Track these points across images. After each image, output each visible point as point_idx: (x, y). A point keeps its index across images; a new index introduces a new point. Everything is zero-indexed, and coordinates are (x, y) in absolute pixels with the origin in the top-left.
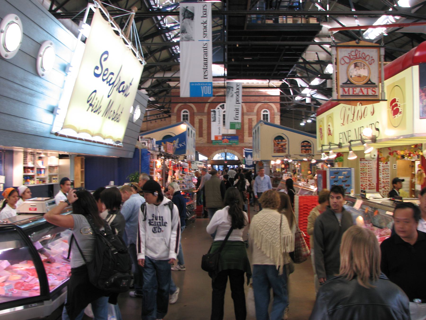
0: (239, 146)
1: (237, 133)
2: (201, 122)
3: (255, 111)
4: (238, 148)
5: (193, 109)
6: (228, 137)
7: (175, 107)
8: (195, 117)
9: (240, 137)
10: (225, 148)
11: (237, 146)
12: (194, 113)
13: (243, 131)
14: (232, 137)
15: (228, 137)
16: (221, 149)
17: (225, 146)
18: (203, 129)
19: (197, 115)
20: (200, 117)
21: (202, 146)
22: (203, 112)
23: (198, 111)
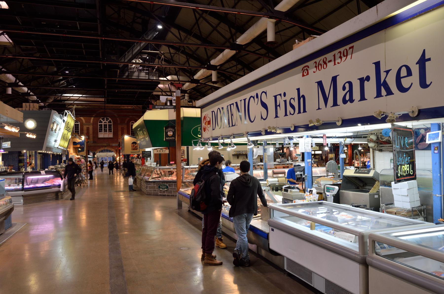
2: (88, 129)
3: (126, 122)
20: (87, 126)
23: (86, 122)
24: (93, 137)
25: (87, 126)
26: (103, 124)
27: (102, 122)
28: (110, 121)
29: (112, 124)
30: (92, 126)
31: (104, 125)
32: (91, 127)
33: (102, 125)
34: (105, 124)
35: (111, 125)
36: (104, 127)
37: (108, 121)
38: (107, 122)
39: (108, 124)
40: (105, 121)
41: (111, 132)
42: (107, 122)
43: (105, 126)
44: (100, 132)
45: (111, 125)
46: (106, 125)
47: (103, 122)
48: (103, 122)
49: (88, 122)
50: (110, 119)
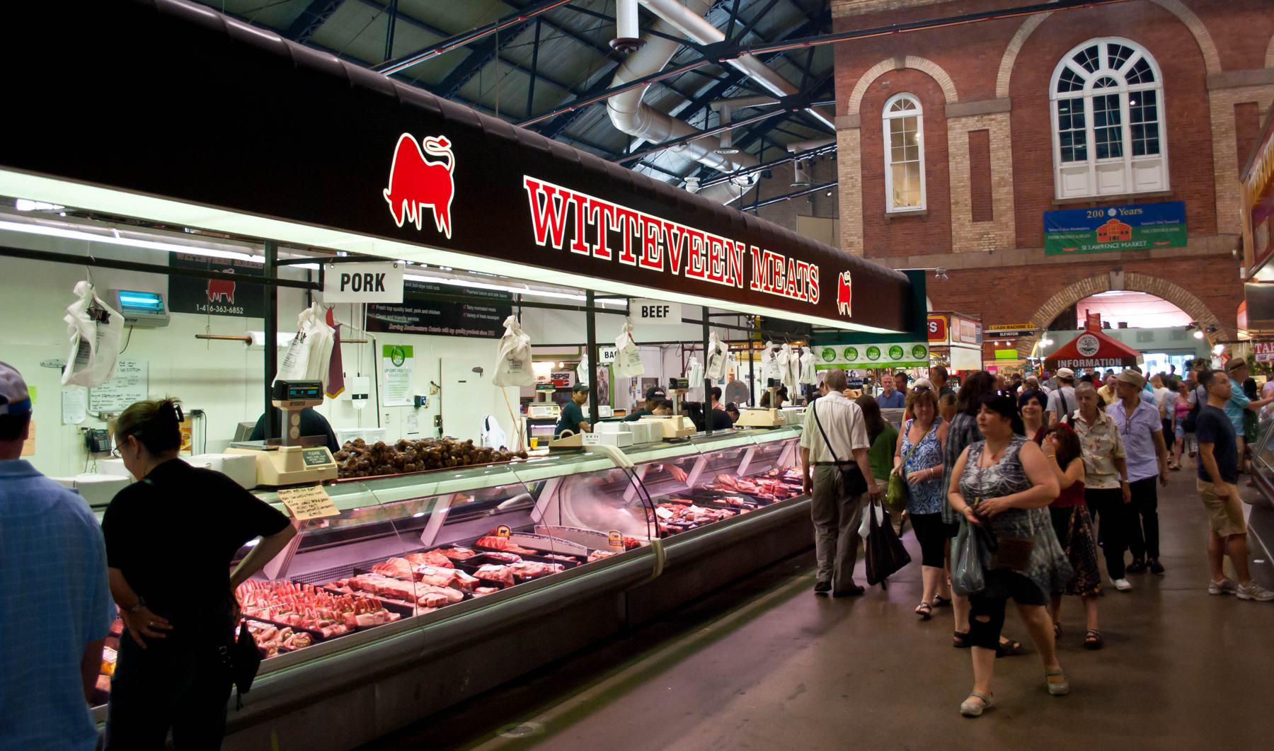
0: (1188, 251)
1: (1172, 185)
2: (979, 145)
4: (1184, 265)
5: (938, 87)
6: (1123, 212)
7: (851, 87)
8: (950, 123)
9: (1193, 208)
10: (1117, 271)
11: (1177, 252)
12: (944, 102)
13: (1212, 170)
14: (1144, 209)
15: (1123, 212)
16: (1093, 275)
17: (1116, 256)
18: (995, 178)
19: (958, 117)
20: (973, 124)
21: (993, 262)
22: (991, 94)
23: (963, 94)
24: (1020, 202)
25: (973, 124)
26: (1088, 94)
27: (1079, 83)
28: (1142, 64)
29: (1157, 85)
30: (1004, 118)
31: (1098, 101)
32: (999, 129)
33: (1079, 103)
34: (1106, 91)
35: (1150, 96)
36: (1099, 119)
37: (1079, 70)
38: (1119, 75)
39: (1123, 89)
40: (1104, 70)
41: (1154, 148)
42: (1119, 75)
43: (1106, 106)
44: (1066, 155)
45: (1150, 96)
46: (1114, 100)
47: (1090, 78)
48: (1090, 78)
49: (977, 91)
50: (1139, 52)
